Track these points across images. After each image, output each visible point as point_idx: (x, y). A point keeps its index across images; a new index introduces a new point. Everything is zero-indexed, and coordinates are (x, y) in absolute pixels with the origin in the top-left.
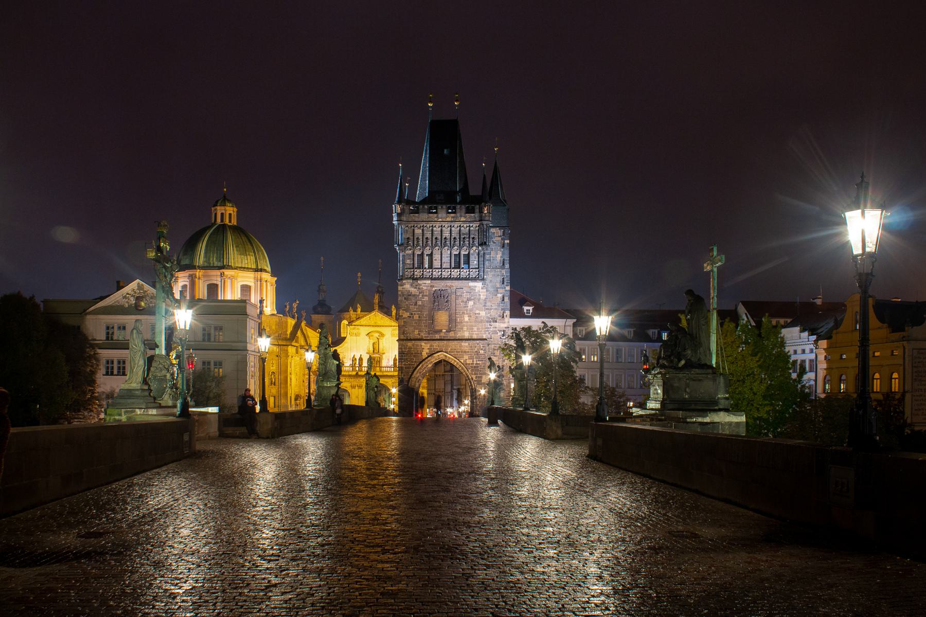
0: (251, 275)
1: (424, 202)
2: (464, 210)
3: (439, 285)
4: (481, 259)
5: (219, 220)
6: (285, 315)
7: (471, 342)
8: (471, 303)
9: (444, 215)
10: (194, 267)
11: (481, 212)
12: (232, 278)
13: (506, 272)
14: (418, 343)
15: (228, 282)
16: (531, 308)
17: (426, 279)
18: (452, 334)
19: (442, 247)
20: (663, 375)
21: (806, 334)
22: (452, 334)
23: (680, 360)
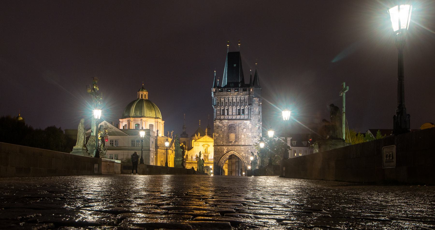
1: (225, 87)
2: (242, 90)
3: (231, 122)
4: (249, 111)
5: (140, 97)
6: (167, 137)
7: (245, 147)
8: (245, 130)
9: (234, 92)
10: (130, 117)
11: (249, 91)
12: (145, 121)
13: (260, 117)
14: (222, 147)
15: (144, 123)
18: (237, 143)
19: (232, 106)
22: (237, 143)
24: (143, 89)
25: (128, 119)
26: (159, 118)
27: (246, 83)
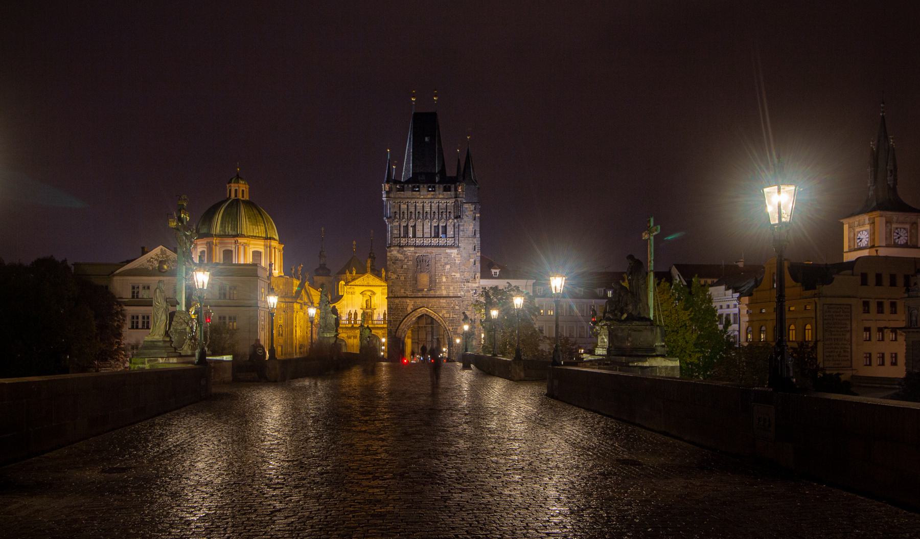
0: (262, 242)
1: (408, 182)
2: (442, 189)
3: (422, 252)
6: (291, 276)
7: (448, 299)
8: (448, 267)
11: (456, 190)
12: (245, 245)
13: (477, 241)
14: (404, 300)
15: (242, 249)
16: (498, 271)
17: (410, 246)
20: (609, 327)
21: (730, 291)
22: (432, 293)
23: (622, 314)
24: (238, 178)
25: (209, 240)
26: (274, 239)
27: (448, 175)
